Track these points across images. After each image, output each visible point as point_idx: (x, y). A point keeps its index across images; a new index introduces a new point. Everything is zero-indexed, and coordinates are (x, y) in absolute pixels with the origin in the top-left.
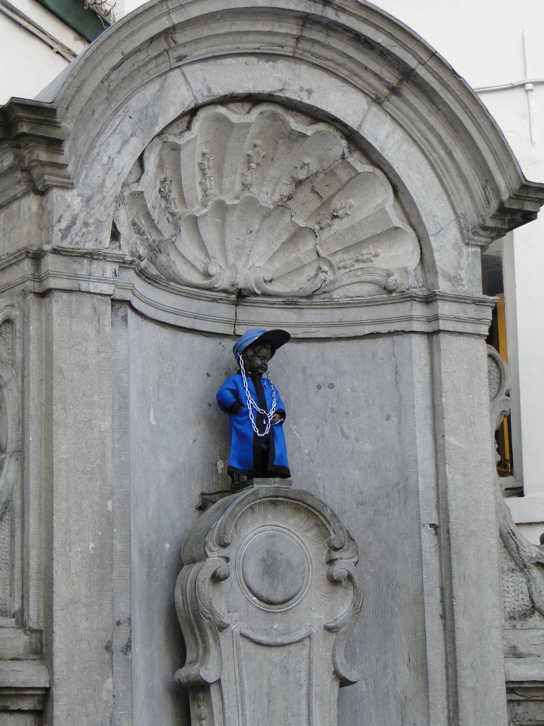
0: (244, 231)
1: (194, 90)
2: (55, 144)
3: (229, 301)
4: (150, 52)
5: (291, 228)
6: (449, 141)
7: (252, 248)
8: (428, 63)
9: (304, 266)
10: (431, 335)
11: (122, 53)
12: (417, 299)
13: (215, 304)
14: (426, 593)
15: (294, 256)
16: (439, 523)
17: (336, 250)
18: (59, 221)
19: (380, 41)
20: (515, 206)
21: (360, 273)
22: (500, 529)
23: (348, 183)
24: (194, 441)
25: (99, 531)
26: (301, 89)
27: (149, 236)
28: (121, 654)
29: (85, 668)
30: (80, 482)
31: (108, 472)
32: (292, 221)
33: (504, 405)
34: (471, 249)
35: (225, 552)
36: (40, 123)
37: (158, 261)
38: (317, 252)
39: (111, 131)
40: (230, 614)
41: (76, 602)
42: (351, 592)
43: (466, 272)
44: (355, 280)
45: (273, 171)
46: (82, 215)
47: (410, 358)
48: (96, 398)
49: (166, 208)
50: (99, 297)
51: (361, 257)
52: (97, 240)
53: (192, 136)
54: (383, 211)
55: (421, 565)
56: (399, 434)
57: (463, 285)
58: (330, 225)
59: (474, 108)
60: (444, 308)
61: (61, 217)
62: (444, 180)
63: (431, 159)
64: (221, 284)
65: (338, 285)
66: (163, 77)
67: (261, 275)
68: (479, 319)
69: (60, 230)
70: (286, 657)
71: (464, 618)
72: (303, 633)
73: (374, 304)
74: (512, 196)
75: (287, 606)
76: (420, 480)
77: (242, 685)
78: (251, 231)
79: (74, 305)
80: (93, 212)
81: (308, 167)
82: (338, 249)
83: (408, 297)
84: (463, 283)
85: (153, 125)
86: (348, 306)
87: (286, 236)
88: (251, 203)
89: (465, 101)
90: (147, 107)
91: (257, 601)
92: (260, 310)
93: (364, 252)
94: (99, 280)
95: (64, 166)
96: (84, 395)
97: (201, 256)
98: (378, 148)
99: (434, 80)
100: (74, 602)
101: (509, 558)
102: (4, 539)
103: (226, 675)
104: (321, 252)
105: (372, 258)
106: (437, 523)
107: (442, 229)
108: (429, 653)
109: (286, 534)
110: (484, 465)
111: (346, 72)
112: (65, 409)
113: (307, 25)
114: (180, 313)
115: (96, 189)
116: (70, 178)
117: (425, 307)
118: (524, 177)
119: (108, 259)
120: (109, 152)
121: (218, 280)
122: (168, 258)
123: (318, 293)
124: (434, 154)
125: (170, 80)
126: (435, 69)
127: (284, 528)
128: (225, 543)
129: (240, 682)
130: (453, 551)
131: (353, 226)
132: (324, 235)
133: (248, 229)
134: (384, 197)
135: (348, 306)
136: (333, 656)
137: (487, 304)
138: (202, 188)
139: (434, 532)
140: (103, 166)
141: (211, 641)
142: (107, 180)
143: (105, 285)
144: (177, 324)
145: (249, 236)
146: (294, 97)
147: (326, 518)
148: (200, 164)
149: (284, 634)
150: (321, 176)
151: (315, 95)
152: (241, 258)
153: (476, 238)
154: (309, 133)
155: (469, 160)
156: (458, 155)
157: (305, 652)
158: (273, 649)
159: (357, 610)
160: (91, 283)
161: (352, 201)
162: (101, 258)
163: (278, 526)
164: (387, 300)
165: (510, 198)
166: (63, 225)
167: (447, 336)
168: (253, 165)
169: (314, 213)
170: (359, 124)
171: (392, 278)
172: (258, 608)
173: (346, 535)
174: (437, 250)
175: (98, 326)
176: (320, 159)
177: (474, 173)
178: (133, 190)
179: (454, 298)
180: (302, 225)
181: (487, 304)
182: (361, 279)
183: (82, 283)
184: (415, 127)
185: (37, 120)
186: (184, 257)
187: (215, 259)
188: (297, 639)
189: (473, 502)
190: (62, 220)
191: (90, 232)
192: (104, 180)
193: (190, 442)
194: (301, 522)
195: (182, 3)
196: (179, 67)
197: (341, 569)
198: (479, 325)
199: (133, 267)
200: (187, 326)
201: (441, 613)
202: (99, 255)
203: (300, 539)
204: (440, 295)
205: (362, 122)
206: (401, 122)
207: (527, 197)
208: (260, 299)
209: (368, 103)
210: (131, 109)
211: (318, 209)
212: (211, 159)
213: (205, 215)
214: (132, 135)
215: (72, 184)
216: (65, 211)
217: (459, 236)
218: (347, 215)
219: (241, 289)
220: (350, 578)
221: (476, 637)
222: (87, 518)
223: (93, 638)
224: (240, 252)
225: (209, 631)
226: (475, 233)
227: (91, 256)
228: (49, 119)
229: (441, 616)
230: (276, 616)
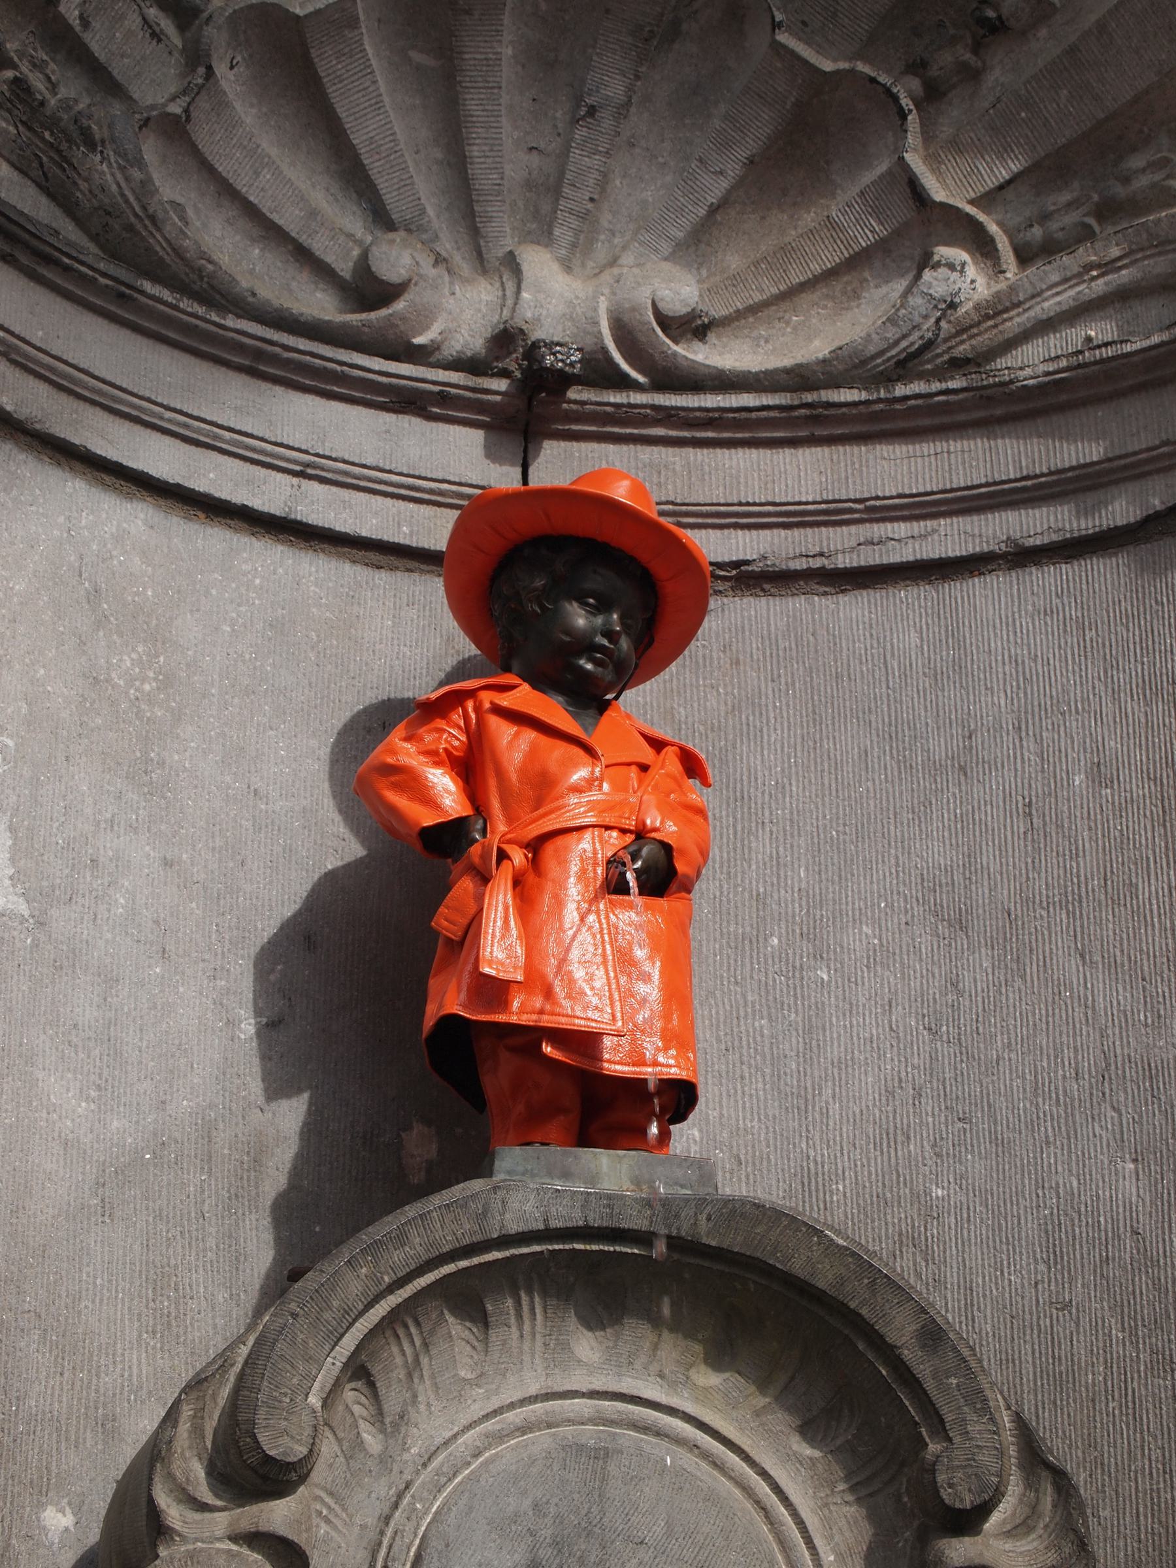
27: (37, 82)
37: (84, 186)
51: (1120, 191)
58: (972, 75)
65: (1016, 322)
78: (592, 111)
92: (647, 453)
93: (1136, 162)
97: (352, 221)
109: (680, 1441)
114: (216, 437)
121: (425, 318)
122: (136, 174)
127: (671, 1411)
128: (269, 1459)
131: (1072, 51)
133: (578, 100)
145: (580, 133)
152: (550, 233)
173: (1009, 1437)
180: (828, 66)
186: (251, 211)
200: (257, 503)
203: (764, 1474)
208: (637, 398)
219: (535, 345)
224: (545, 208)
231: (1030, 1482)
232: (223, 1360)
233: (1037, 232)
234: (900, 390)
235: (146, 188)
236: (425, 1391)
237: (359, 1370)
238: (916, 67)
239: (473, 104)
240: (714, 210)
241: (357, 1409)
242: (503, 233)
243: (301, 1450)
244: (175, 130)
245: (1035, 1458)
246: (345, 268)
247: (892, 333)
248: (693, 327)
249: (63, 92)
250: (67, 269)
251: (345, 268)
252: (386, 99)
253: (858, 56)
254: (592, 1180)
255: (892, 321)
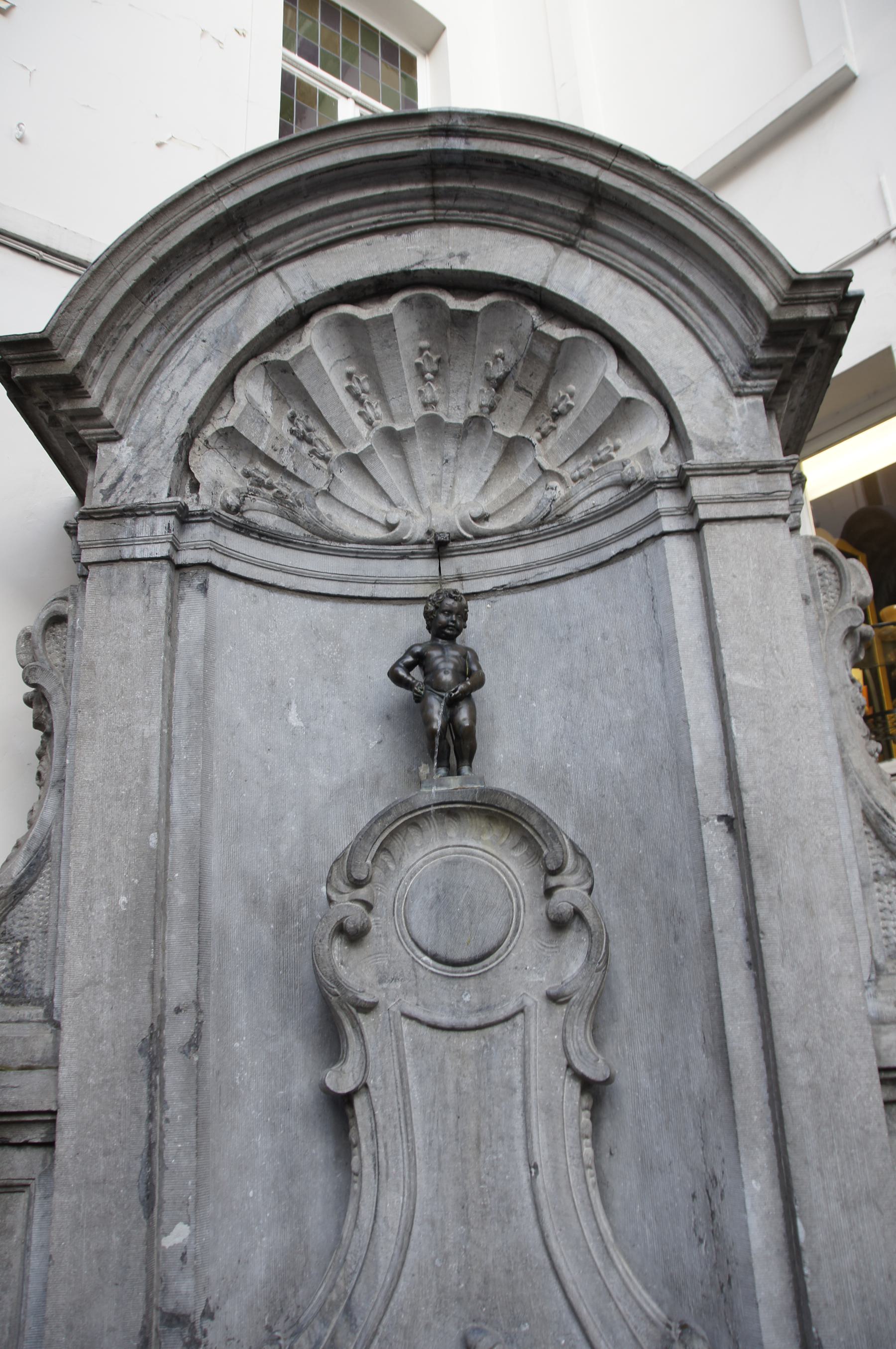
0: (439, 463)
1: (292, 289)
2: (72, 385)
3: (424, 554)
4: (213, 256)
5: (498, 443)
6: (677, 263)
7: (454, 481)
8: (615, 164)
9: (528, 490)
10: (695, 532)
11: (154, 258)
12: (663, 486)
13: (406, 561)
14: (717, 927)
15: (514, 480)
16: (735, 813)
17: (566, 457)
18: (101, 481)
19: (536, 157)
20: (791, 314)
21: (597, 477)
22: (863, 811)
23: (553, 361)
24: (379, 743)
25: (135, 878)
26: (451, 256)
27: (284, 491)
28: (181, 1057)
29: (105, 1081)
30: (109, 812)
31: (151, 794)
32: (494, 433)
33: (849, 619)
34: (745, 401)
35: (362, 893)
36: (37, 361)
38: (539, 465)
39: (177, 363)
40: (385, 985)
41: (97, 984)
42: (585, 938)
43: (740, 433)
44: (594, 488)
45: (456, 377)
46: (131, 468)
47: (666, 572)
48: (139, 695)
49: (313, 452)
50: (151, 562)
51: (598, 458)
52: (150, 493)
53: (303, 348)
54: (604, 382)
55: (706, 884)
56: (664, 686)
57: (739, 452)
58: (554, 429)
59: (697, 201)
60: (700, 487)
61: (104, 475)
62: (687, 318)
63: (662, 295)
64: (413, 534)
65: (573, 502)
66: (251, 287)
67: (467, 512)
68: (768, 494)
69: (101, 491)
70: (486, 1046)
71: (783, 966)
72: (511, 1007)
73: (615, 511)
74: (781, 302)
75: (484, 967)
76: (695, 750)
77: (405, 1092)
78: (447, 461)
79: (116, 578)
80: (146, 460)
81: (503, 359)
82: (569, 455)
83: (649, 487)
84: (738, 448)
85: (234, 343)
86: (585, 524)
87: (495, 457)
88: (433, 424)
89: (680, 195)
90: (227, 324)
91: (431, 962)
92: (474, 558)
93: (601, 448)
94: (147, 542)
95: (97, 413)
96: (122, 692)
97: (385, 506)
98: (575, 300)
99: (629, 184)
100: (93, 983)
101: (886, 855)
102: (42, 899)
103: (379, 1078)
104: (546, 466)
105: (613, 453)
106: (731, 813)
107: (693, 383)
108: (729, 1028)
110: (802, 711)
111: (513, 219)
112: (94, 715)
113: (438, 172)
115: (152, 433)
116: (112, 427)
117: (680, 495)
118: (794, 270)
119: (157, 512)
120: (172, 388)
121: (406, 531)
122: (314, 510)
123: (550, 518)
124: (663, 287)
125: (259, 287)
126: (626, 168)
129: (403, 1089)
130: (753, 856)
131: (578, 418)
132: (551, 442)
133: (443, 459)
134: (609, 367)
135: (585, 524)
136: (564, 1041)
137: (778, 469)
138: (365, 421)
139: (726, 828)
140: (165, 403)
141: (349, 1028)
142: (168, 419)
143: (156, 545)
144: (345, 593)
145: (445, 468)
146: (439, 266)
147: (531, 826)
148: (349, 389)
149: (480, 1010)
150: (521, 364)
151: (472, 258)
153: (749, 383)
154: (477, 309)
155: (713, 277)
156: (696, 277)
157: (517, 1037)
158: (463, 1034)
159: (600, 962)
160: (137, 547)
161: (572, 387)
162: (147, 512)
163: (466, 846)
164: (628, 500)
165: (780, 306)
166: (106, 484)
167: (717, 527)
168: (429, 376)
169: (528, 417)
170: (543, 276)
171: (628, 466)
172: (432, 972)
174: (686, 412)
175: (147, 600)
176: (514, 343)
177: (724, 293)
178: (217, 428)
179: (718, 469)
180: (510, 435)
181: (778, 469)
182: (600, 485)
183: (125, 548)
184: (630, 260)
185: (32, 358)
186: (353, 510)
187: (403, 505)
188: (501, 1017)
189: (787, 772)
190: (105, 479)
191: (141, 486)
192: (164, 421)
193: (372, 744)
194: (503, 836)
195: (233, 182)
196: (271, 269)
197: (562, 902)
198: (771, 503)
199: (208, 518)
200: (362, 594)
201: (749, 958)
202: (143, 508)
203: (503, 863)
204: (689, 470)
205: (548, 273)
206: (608, 261)
207: (807, 298)
208: (468, 543)
209: (555, 250)
210: (205, 332)
211: (532, 411)
212: (361, 379)
213: (369, 451)
214: (204, 361)
215: (117, 433)
216: (109, 467)
217: (723, 388)
218: (570, 407)
220: (577, 913)
221: (810, 996)
222: (118, 860)
223: (120, 1036)
224: (439, 491)
225: (342, 1015)
226: (746, 377)
227: (133, 512)
228: (45, 353)
229: (749, 964)
230: (465, 983)
231: (576, 859)
232: (343, 854)
233: (577, 473)
234: (541, 528)
235: (318, 513)
236: (406, 851)
237: (383, 848)
238: (538, 429)
239: (413, 466)
240: (486, 483)
241: (386, 860)
242: (427, 502)
243: (365, 876)
244: (327, 493)
245: (578, 853)
246: (382, 521)
247: (538, 511)
248: (484, 518)
249: (294, 491)
250: (295, 543)
251: (382, 521)
252: (388, 470)
253: (521, 430)
254: (448, 786)
255: (537, 507)
